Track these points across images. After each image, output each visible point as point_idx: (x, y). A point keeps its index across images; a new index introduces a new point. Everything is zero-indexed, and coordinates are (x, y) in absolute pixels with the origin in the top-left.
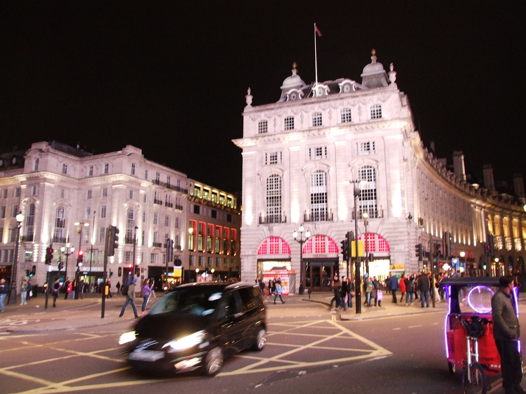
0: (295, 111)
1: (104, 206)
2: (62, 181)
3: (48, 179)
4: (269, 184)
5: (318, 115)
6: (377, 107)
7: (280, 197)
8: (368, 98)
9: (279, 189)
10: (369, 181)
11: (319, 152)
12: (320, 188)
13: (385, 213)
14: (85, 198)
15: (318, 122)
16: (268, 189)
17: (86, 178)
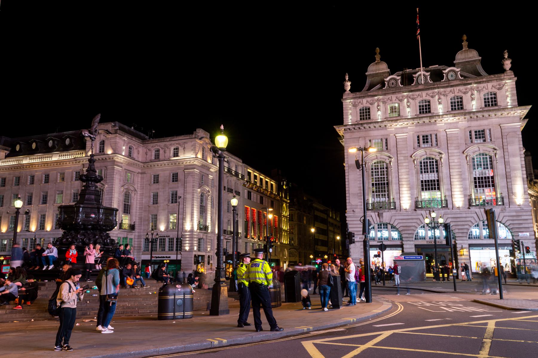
0: (401, 98)
1: (184, 191)
2: (129, 164)
3: (117, 162)
4: (374, 170)
5: (426, 102)
6: (426, 102)
7: (388, 184)
8: (482, 85)
9: (385, 176)
10: (484, 168)
11: (426, 139)
12: (430, 175)
13: (506, 201)
14: (151, 182)
15: (425, 109)
16: (372, 175)
17: (151, 161)
